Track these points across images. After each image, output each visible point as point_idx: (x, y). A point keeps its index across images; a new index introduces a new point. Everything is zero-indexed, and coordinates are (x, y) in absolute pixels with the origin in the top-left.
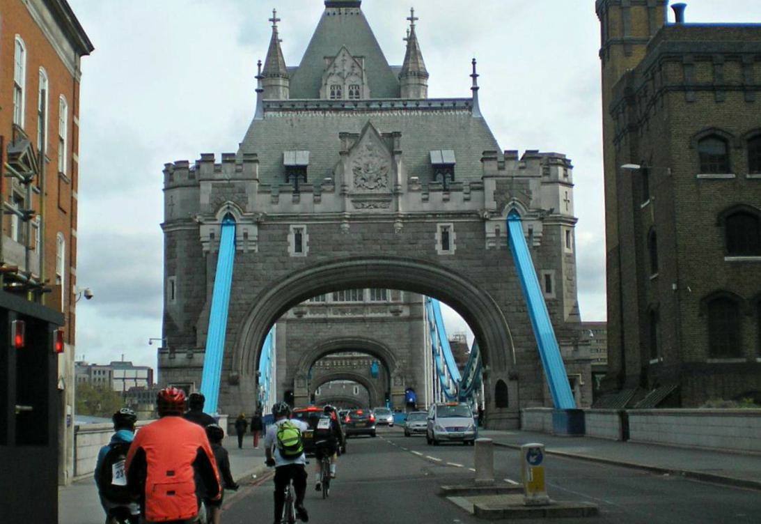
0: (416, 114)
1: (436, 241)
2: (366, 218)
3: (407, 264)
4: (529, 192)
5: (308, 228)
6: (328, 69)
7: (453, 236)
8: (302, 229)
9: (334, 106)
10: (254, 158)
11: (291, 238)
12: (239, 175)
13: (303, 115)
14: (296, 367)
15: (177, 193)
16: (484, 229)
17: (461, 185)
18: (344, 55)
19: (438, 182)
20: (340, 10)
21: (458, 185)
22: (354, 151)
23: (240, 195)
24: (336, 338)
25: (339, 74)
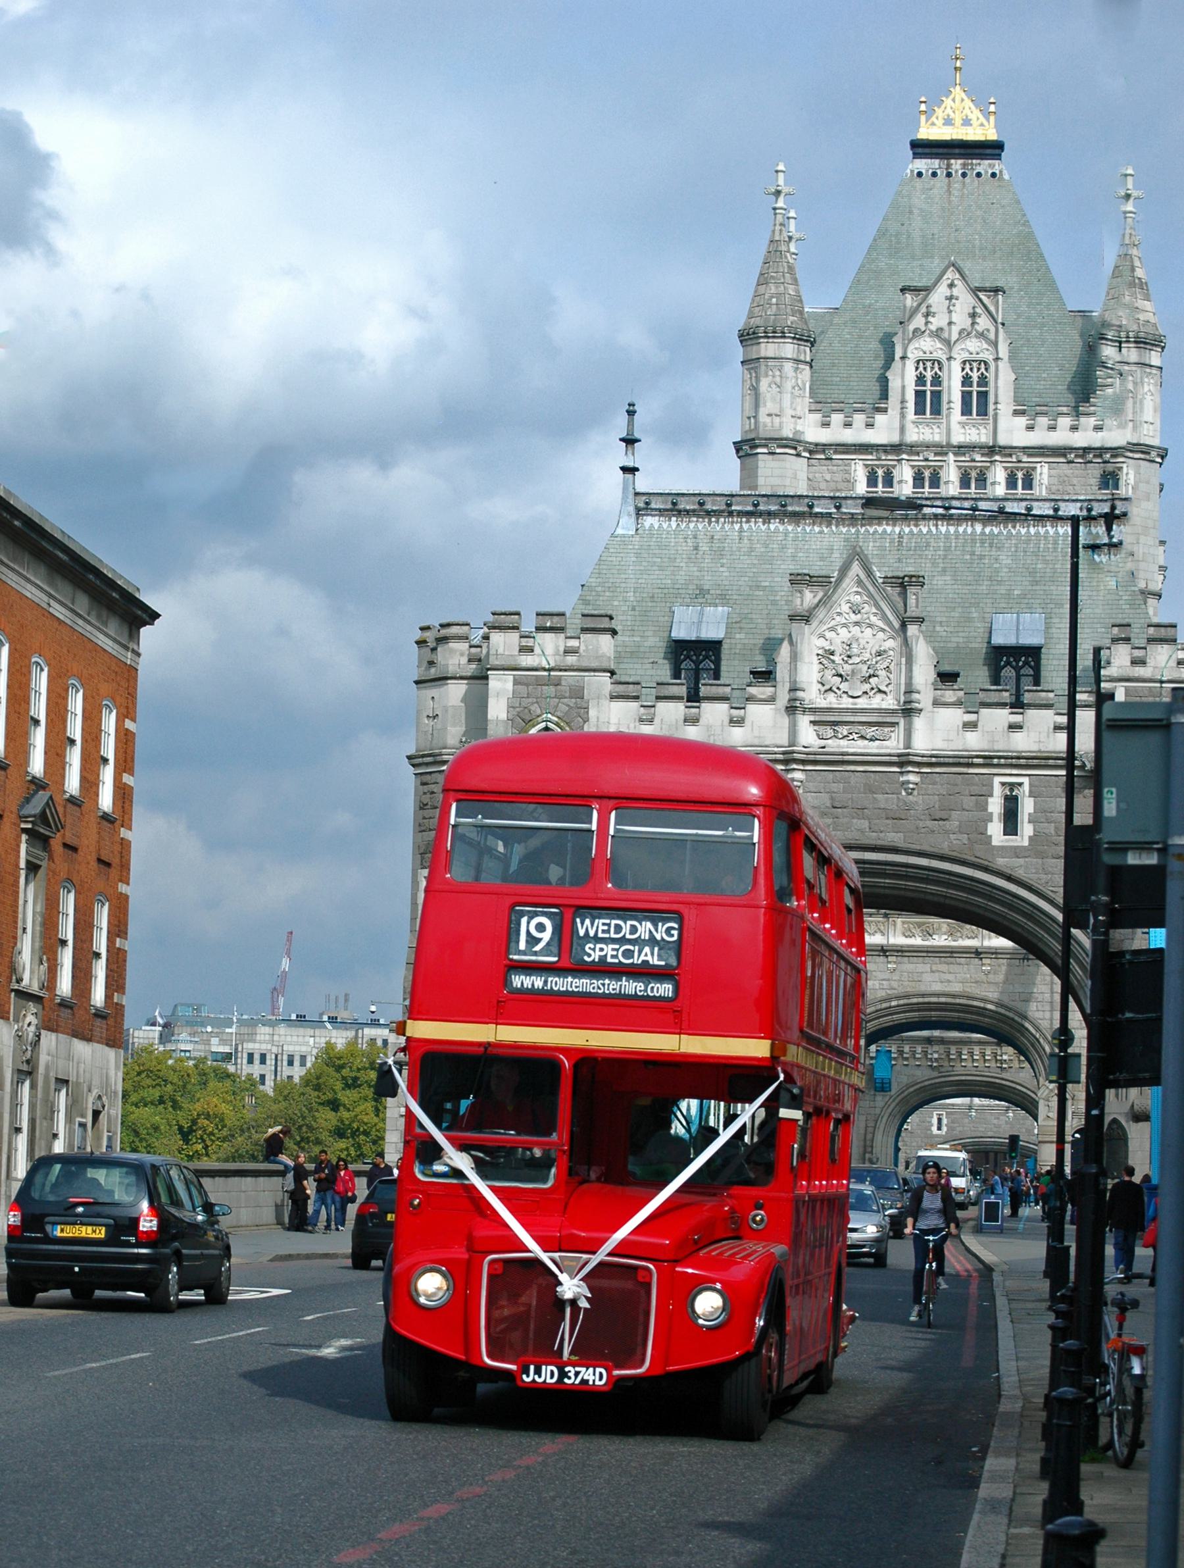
0: (969, 530)
2: (841, 760)
3: (924, 862)
6: (911, 317)
7: (1027, 806)
9: (790, 508)
10: (605, 623)
12: (571, 660)
17: (1051, 695)
18: (951, 286)
20: (949, 166)
21: (1043, 694)
22: (821, 613)
24: (907, 996)
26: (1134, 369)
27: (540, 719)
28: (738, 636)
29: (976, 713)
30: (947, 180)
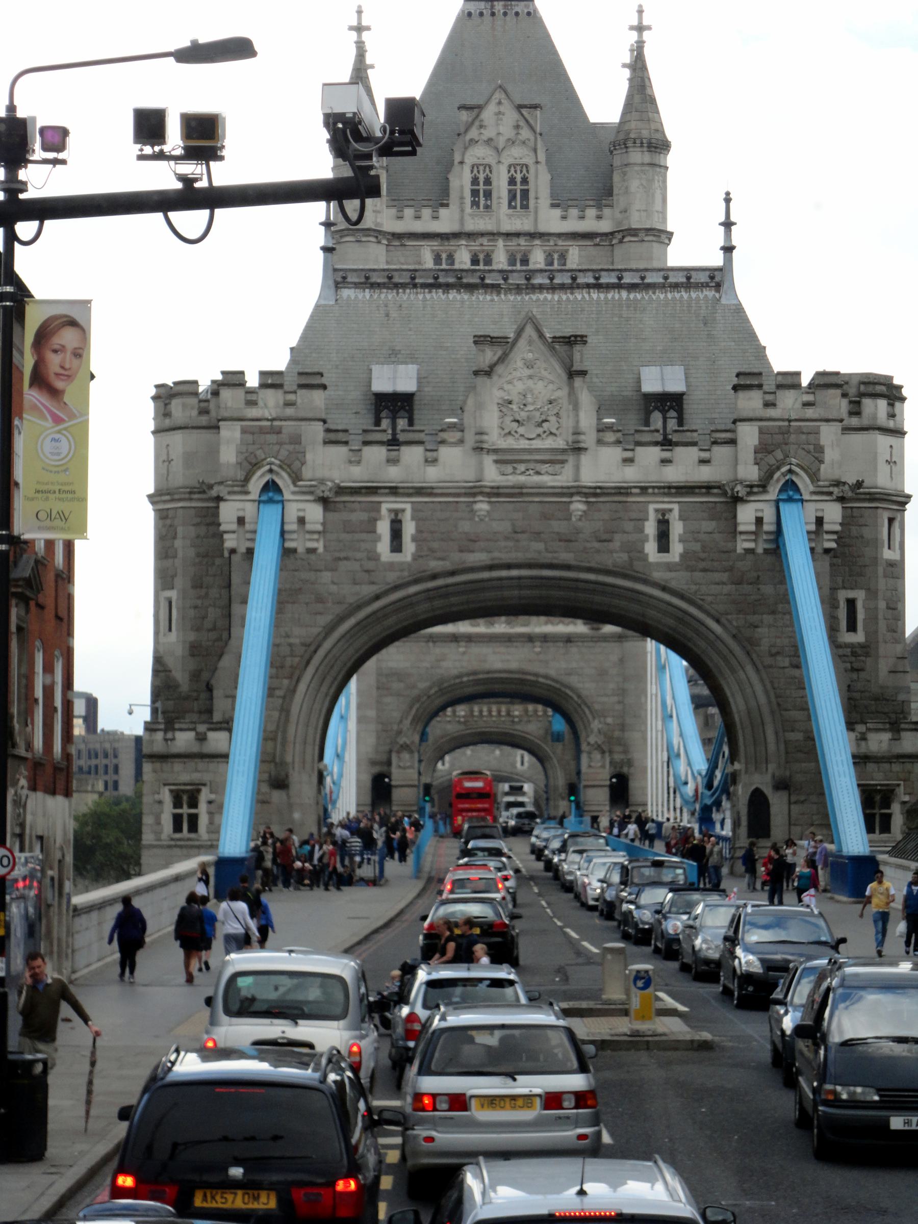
0: (617, 296)
1: (647, 536)
2: (518, 492)
3: (591, 577)
4: (820, 449)
5: (414, 510)
6: (467, 131)
7: (677, 528)
8: (403, 510)
9: (465, 281)
11: (384, 528)
12: (289, 411)
13: (407, 296)
14: (395, 727)
15: (177, 438)
16: (735, 517)
17: (695, 434)
18: (500, 103)
19: (652, 428)
20: (492, 7)
21: (689, 434)
22: (500, 369)
23: (291, 447)
24: (475, 673)
25: (489, 141)
26: (647, 168)
27: (265, 462)
28: (426, 389)
29: (633, 450)
30: (491, 18)
